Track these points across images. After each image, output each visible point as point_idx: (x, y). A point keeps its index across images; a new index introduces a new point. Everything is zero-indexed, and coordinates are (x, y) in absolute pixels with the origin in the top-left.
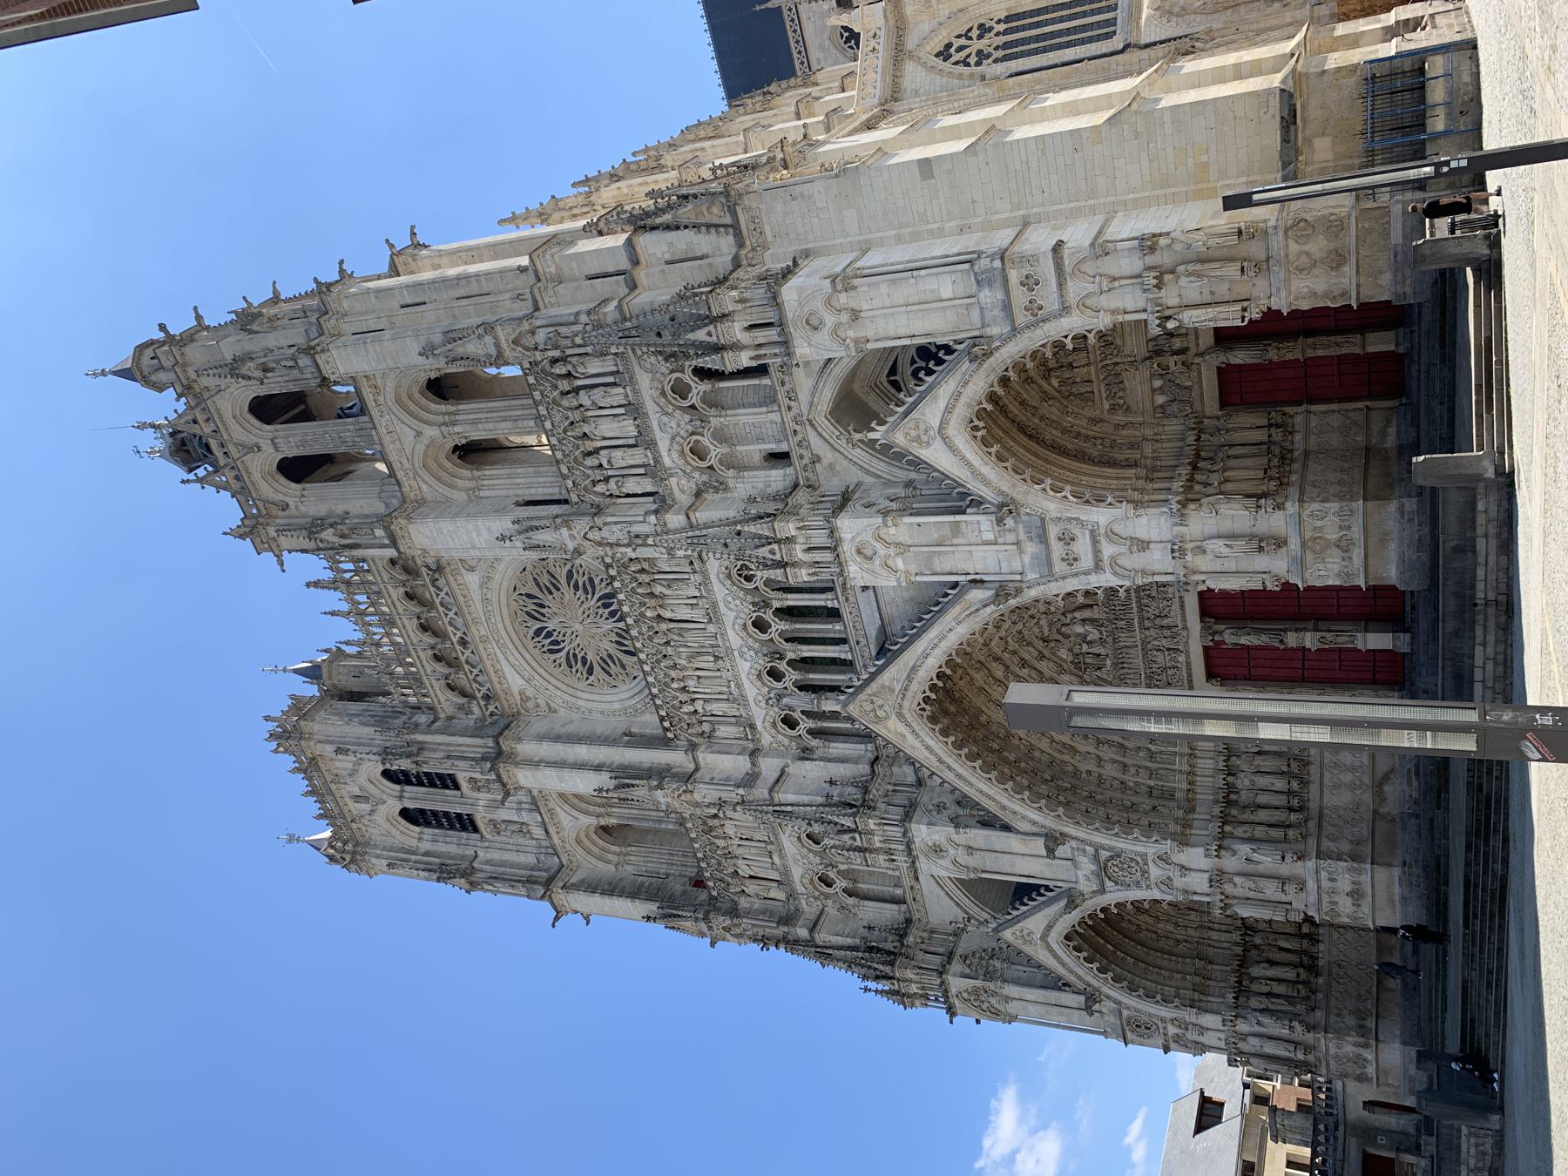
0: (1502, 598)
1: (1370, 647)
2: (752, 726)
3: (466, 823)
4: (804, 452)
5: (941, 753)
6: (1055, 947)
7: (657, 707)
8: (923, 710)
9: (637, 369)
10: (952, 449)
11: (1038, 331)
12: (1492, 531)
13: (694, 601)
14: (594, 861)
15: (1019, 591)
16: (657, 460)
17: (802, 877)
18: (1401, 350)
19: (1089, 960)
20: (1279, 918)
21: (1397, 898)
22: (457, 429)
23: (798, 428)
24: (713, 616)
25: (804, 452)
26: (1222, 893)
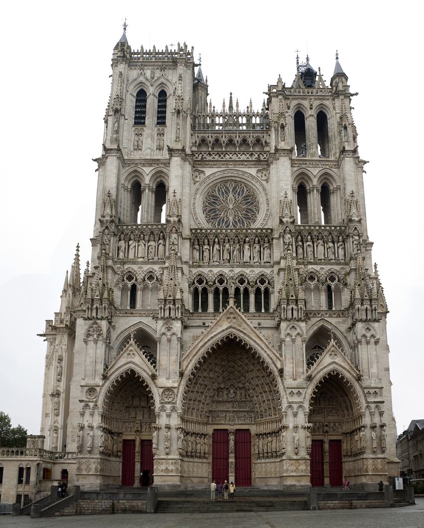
1: (230, 477)
2: (200, 266)
3: (140, 120)
6: (128, 366)
7: (206, 230)
9: (341, 266)
13: (252, 259)
14: (126, 174)
15: (281, 377)
16: (311, 263)
17: (133, 269)
19: (121, 377)
20: (154, 446)
22: (315, 191)
23: (320, 315)
24: (245, 265)
25: (312, 314)
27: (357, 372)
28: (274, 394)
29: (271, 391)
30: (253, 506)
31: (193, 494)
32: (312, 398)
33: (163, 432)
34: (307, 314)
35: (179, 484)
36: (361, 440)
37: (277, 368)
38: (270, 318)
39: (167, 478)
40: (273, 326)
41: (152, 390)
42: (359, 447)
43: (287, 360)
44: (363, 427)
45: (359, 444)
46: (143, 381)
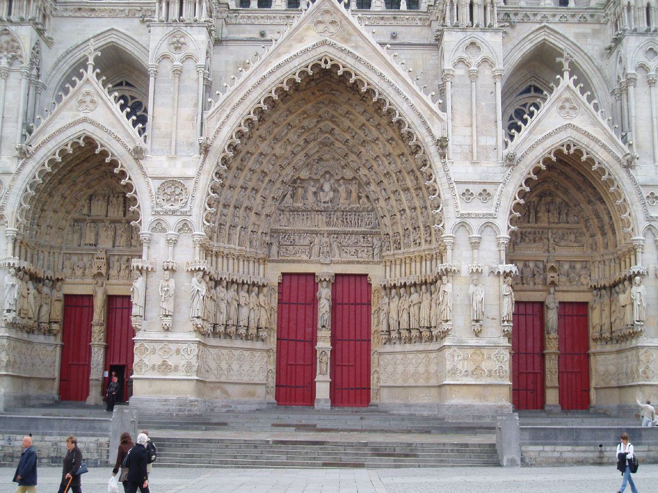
0: (605, 460)
4: (520, 17)
5: (286, 68)
8: (326, 62)
10: (558, 131)
11: (635, 198)
12: (651, 454)
15: (443, 156)
18: (546, 408)
19: (63, 152)
20: (135, 310)
21: (164, 397)
23: (538, 18)
25: (520, 17)
26: (152, 269)
27: (626, 147)
28: (426, 194)
29: (420, 189)
30: (365, 455)
31: (225, 424)
32: (517, 207)
33: (158, 281)
34: (507, 15)
35: (193, 398)
36: (633, 304)
37: (433, 136)
38: (420, 23)
39: (167, 385)
40: (426, 42)
41: (134, 182)
42: (628, 320)
43: (458, 119)
44: (638, 274)
45: (628, 316)
46: (114, 164)
